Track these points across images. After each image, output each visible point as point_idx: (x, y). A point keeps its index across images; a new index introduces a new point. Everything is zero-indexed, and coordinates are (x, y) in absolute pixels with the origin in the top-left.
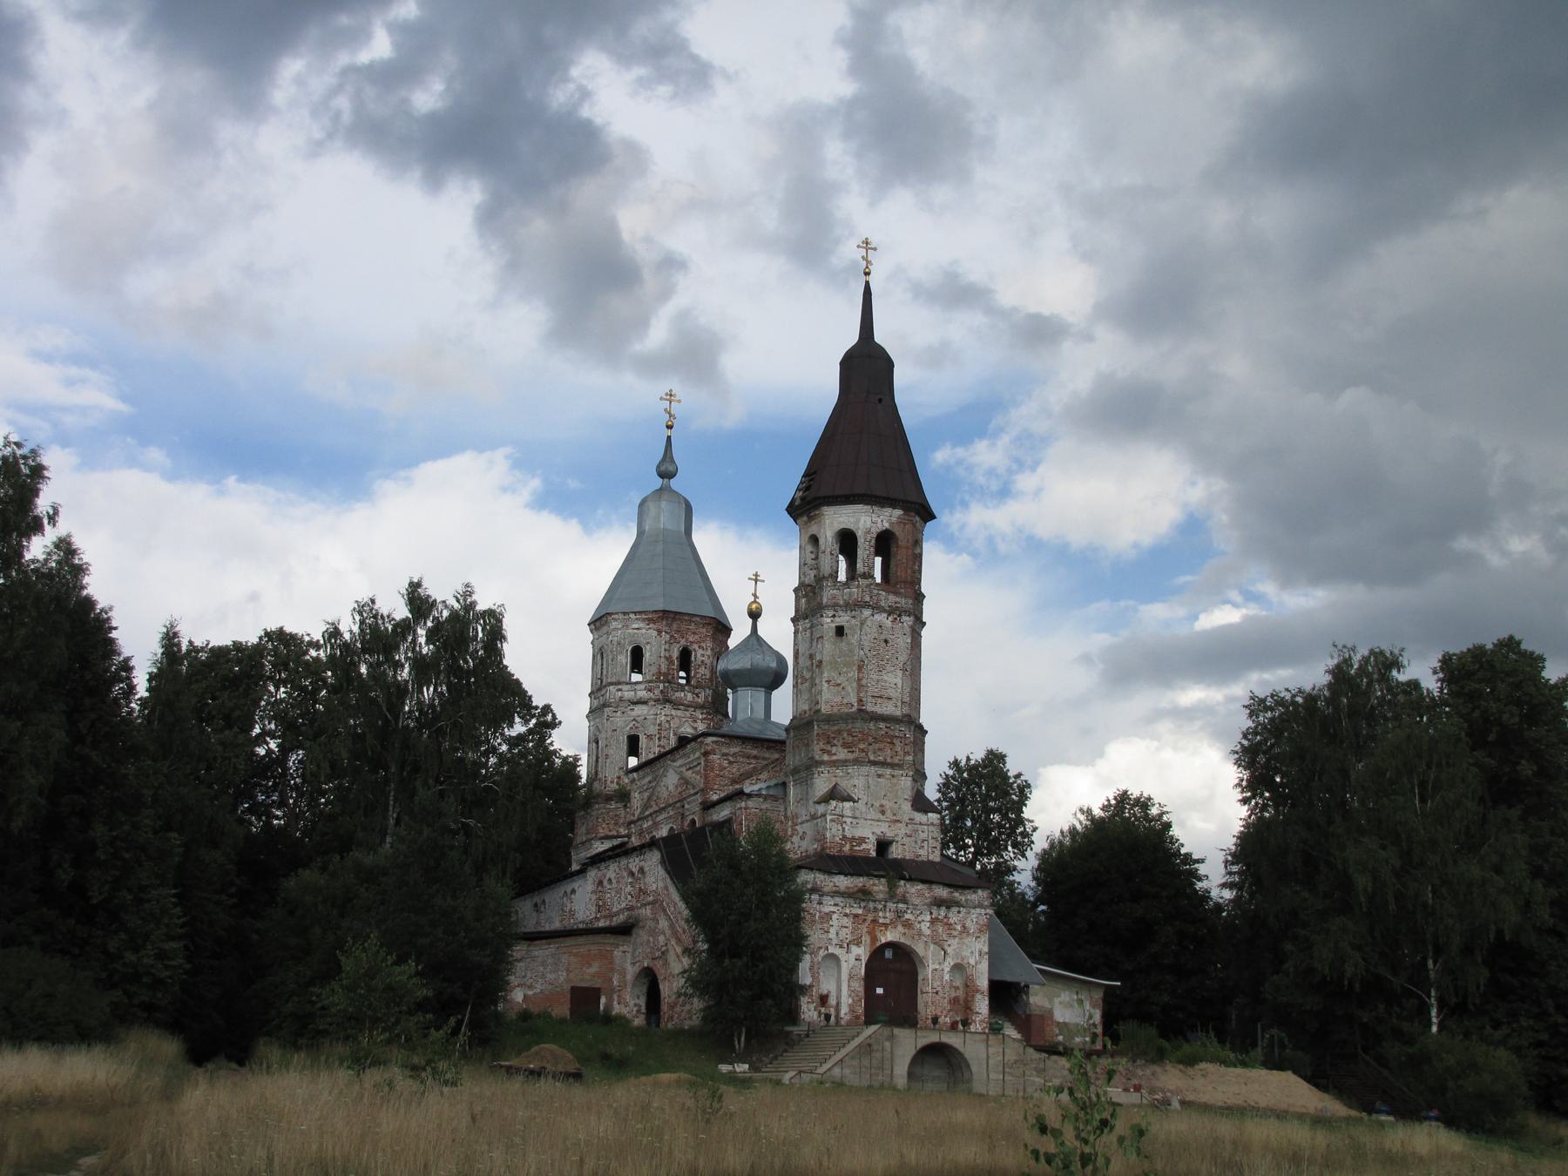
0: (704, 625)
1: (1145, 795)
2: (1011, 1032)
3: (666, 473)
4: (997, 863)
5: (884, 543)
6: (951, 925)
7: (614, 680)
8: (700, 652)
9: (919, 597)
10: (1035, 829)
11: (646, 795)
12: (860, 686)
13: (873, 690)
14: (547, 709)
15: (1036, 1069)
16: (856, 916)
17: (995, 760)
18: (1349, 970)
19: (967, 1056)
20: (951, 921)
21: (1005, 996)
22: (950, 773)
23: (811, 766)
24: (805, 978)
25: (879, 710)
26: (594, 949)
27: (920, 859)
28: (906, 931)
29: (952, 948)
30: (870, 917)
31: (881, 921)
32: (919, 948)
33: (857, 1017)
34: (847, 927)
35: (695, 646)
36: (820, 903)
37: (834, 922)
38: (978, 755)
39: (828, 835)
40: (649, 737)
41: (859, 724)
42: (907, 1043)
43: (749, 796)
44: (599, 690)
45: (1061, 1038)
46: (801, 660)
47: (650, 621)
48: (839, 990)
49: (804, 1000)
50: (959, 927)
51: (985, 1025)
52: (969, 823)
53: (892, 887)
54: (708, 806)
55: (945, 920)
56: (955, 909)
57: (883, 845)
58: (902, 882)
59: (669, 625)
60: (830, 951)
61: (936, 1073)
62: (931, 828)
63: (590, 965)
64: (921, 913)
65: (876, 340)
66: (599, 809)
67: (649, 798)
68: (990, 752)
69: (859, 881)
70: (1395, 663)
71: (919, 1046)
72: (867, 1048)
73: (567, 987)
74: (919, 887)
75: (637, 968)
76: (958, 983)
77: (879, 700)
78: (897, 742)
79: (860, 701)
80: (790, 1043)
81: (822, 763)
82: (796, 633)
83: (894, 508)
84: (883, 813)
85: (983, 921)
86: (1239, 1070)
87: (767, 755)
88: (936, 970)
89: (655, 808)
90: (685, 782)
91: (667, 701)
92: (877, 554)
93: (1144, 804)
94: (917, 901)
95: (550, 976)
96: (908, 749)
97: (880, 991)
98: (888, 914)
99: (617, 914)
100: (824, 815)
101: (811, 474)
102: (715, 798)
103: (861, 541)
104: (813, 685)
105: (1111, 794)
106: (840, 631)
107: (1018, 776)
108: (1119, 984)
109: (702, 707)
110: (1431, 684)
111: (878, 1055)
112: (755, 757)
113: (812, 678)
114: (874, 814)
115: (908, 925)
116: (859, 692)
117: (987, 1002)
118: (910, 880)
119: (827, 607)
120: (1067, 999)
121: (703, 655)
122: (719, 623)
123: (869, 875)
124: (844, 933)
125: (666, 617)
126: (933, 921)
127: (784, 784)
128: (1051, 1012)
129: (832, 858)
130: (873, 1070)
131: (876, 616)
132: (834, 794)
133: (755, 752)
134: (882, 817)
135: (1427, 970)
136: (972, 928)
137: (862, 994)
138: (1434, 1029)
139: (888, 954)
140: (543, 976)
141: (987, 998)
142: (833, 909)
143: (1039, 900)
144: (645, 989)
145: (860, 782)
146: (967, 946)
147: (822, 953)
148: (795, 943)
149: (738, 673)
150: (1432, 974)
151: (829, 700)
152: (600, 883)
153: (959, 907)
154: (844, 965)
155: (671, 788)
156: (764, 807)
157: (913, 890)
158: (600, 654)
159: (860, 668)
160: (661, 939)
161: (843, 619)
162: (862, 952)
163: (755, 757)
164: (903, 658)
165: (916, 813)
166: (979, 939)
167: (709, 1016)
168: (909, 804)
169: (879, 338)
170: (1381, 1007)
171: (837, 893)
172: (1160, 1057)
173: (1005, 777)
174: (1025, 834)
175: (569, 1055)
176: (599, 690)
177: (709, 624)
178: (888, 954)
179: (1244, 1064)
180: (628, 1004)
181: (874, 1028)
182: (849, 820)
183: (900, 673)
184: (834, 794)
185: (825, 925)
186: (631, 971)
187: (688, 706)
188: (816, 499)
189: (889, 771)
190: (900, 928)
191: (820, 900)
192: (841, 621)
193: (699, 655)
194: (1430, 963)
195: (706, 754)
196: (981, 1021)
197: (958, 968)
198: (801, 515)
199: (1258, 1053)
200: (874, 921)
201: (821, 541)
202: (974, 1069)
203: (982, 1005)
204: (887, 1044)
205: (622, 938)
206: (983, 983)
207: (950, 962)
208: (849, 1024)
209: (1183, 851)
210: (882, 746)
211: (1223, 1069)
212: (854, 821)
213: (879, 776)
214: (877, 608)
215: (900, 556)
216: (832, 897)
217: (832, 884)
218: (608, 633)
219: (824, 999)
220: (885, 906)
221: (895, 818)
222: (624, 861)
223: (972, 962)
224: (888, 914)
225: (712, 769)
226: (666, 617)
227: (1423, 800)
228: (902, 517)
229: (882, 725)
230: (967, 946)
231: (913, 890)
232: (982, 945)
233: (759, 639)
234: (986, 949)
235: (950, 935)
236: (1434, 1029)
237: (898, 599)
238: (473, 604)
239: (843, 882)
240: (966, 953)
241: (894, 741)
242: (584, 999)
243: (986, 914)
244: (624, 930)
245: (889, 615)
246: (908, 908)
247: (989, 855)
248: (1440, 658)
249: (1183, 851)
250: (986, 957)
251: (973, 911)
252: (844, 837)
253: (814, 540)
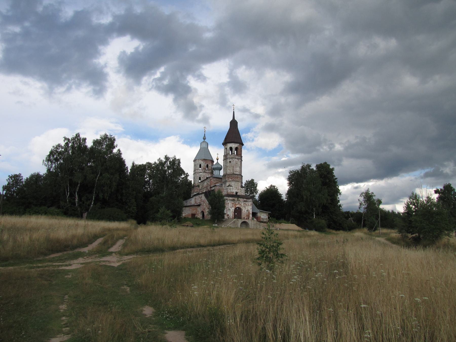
1: (274, 185)
2: (255, 219)
3: (204, 139)
4: (253, 195)
5: (236, 149)
7: (197, 169)
8: (210, 165)
9: (242, 157)
10: (258, 190)
11: (202, 186)
12: (233, 170)
14: (187, 173)
15: (259, 225)
16: (233, 203)
17: (252, 180)
18: (303, 210)
21: (254, 214)
22: (246, 182)
23: (226, 181)
24: (225, 212)
26: (195, 208)
32: (242, 208)
33: (233, 218)
36: (227, 201)
38: (250, 180)
39: (229, 191)
40: (202, 177)
41: (233, 175)
42: (240, 221)
43: (217, 186)
44: (195, 171)
45: (262, 220)
46: (224, 166)
47: (202, 160)
48: (230, 214)
49: (225, 215)
52: (249, 190)
53: (238, 199)
54: (211, 187)
56: (247, 202)
57: (236, 193)
59: (205, 161)
61: (244, 225)
63: (194, 210)
66: (195, 188)
67: (202, 186)
68: (252, 179)
70: (310, 166)
72: (234, 222)
73: (191, 214)
75: (201, 211)
76: (247, 213)
78: (238, 178)
79: (233, 172)
80: (223, 221)
81: (228, 181)
82: (224, 162)
84: (236, 188)
86: (287, 224)
87: (219, 180)
89: (203, 188)
90: (207, 184)
91: (205, 172)
92: (235, 150)
93: (274, 187)
94: (241, 201)
95: (188, 212)
97: (236, 214)
99: (198, 203)
100: (228, 189)
101: (226, 139)
102: (212, 186)
103: (233, 149)
104: (226, 170)
105: (269, 185)
106: (230, 162)
107: (256, 183)
109: (210, 173)
110: (315, 169)
111: (236, 223)
112: (218, 180)
113: (226, 169)
114: (235, 188)
115: (240, 204)
116: (233, 171)
118: (240, 198)
119: (228, 158)
122: (213, 161)
123: (235, 197)
125: (205, 160)
126: (244, 204)
127: (222, 184)
128: (261, 217)
129: (229, 195)
132: (229, 186)
133: (218, 180)
135: (314, 209)
137: (234, 214)
138: (314, 217)
139: (237, 209)
140: (187, 212)
143: (259, 200)
144: (202, 214)
145: (233, 184)
147: (228, 208)
148: (224, 207)
149: (215, 168)
150: (314, 210)
151: (229, 172)
152: (195, 199)
154: (231, 210)
155: (206, 185)
156: (219, 187)
157: (241, 199)
158: (195, 165)
159: (233, 167)
160: (204, 207)
161: (231, 160)
162: (234, 208)
163: (218, 180)
164: (239, 166)
167: (211, 217)
169: (235, 119)
170: (307, 215)
171: (230, 200)
172: (276, 223)
173: (254, 183)
174: (257, 191)
175: (191, 223)
176: (195, 171)
178: (237, 209)
179: (288, 223)
180: (200, 216)
181: (236, 219)
182: (231, 189)
184: (229, 186)
186: (200, 211)
188: (226, 142)
192: (230, 160)
194: (314, 208)
195: (211, 180)
197: (247, 210)
198: (224, 145)
199: (290, 222)
201: (227, 149)
203: (251, 216)
204: (237, 221)
205: (198, 207)
206: (251, 213)
207: (246, 210)
208: (232, 219)
209: (280, 193)
211: (285, 224)
214: (236, 158)
215: (239, 151)
218: (196, 162)
219: (228, 215)
222: (199, 195)
223: (249, 209)
225: (212, 182)
226: (205, 160)
227: (313, 185)
229: (236, 176)
233: (218, 163)
236: (314, 217)
238: (176, 158)
239: (231, 198)
240: (249, 208)
242: (193, 215)
244: (199, 205)
247: (252, 194)
248: (316, 166)
249: (280, 193)
252: (231, 192)
253: (226, 148)
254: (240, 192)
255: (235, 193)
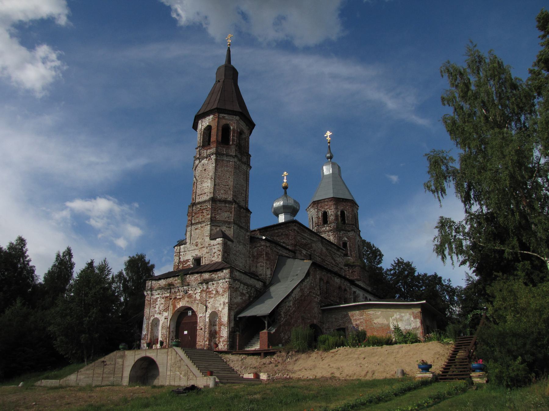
0: (330, 201)
6: (210, 292)
8: (330, 211)
13: (199, 192)
16: (167, 297)
19: (157, 363)
20: (211, 290)
25: (200, 200)
27: (213, 262)
28: (189, 300)
29: (210, 303)
30: (173, 297)
31: (178, 297)
34: (163, 304)
35: (328, 210)
36: (152, 295)
37: (158, 303)
50: (214, 292)
51: (225, 343)
55: (208, 290)
57: (197, 260)
58: (188, 276)
60: (155, 317)
62: (218, 246)
64: (196, 289)
65: (231, 64)
69: (170, 280)
71: (136, 359)
74: (196, 276)
77: (201, 196)
78: (204, 211)
83: (209, 116)
84: (197, 245)
85: (226, 285)
88: (201, 317)
96: (208, 212)
98: (181, 293)
108: (425, 302)
114: (193, 247)
115: (190, 296)
117: (226, 330)
120: (398, 317)
121: (331, 212)
124: (162, 307)
130: (105, 375)
131: (203, 162)
134: (196, 248)
136: (220, 290)
141: (226, 328)
142: (158, 296)
146: (218, 301)
153: (212, 281)
165: (212, 241)
166: (223, 296)
168: (208, 238)
171: (160, 288)
177: (332, 200)
183: (209, 181)
185: (154, 305)
187: (326, 232)
189: (199, 226)
190: (186, 299)
191: (151, 293)
193: (329, 212)
196: (223, 341)
200: (175, 298)
202: (161, 370)
207: (209, 311)
210: (198, 215)
212: (184, 253)
213: (196, 229)
216: (156, 290)
217: (158, 285)
220: (179, 290)
221: (202, 246)
223: (220, 309)
224: (181, 293)
228: (213, 117)
229: (198, 206)
230: (218, 301)
231: (193, 278)
232: (225, 299)
234: (227, 301)
235: (210, 297)
237: (211, 151)
241: (203, 211)
243: (226, 282)
245: (207, 158)
246: (189, 288)
250: (227, 305)
251: (220, 282)
254: (207, 253)
255: (190, 264)
